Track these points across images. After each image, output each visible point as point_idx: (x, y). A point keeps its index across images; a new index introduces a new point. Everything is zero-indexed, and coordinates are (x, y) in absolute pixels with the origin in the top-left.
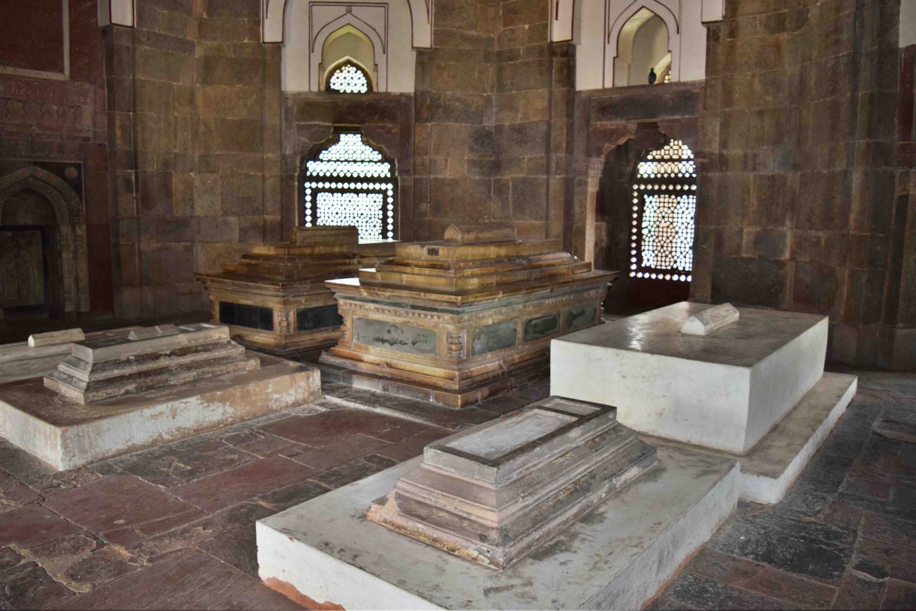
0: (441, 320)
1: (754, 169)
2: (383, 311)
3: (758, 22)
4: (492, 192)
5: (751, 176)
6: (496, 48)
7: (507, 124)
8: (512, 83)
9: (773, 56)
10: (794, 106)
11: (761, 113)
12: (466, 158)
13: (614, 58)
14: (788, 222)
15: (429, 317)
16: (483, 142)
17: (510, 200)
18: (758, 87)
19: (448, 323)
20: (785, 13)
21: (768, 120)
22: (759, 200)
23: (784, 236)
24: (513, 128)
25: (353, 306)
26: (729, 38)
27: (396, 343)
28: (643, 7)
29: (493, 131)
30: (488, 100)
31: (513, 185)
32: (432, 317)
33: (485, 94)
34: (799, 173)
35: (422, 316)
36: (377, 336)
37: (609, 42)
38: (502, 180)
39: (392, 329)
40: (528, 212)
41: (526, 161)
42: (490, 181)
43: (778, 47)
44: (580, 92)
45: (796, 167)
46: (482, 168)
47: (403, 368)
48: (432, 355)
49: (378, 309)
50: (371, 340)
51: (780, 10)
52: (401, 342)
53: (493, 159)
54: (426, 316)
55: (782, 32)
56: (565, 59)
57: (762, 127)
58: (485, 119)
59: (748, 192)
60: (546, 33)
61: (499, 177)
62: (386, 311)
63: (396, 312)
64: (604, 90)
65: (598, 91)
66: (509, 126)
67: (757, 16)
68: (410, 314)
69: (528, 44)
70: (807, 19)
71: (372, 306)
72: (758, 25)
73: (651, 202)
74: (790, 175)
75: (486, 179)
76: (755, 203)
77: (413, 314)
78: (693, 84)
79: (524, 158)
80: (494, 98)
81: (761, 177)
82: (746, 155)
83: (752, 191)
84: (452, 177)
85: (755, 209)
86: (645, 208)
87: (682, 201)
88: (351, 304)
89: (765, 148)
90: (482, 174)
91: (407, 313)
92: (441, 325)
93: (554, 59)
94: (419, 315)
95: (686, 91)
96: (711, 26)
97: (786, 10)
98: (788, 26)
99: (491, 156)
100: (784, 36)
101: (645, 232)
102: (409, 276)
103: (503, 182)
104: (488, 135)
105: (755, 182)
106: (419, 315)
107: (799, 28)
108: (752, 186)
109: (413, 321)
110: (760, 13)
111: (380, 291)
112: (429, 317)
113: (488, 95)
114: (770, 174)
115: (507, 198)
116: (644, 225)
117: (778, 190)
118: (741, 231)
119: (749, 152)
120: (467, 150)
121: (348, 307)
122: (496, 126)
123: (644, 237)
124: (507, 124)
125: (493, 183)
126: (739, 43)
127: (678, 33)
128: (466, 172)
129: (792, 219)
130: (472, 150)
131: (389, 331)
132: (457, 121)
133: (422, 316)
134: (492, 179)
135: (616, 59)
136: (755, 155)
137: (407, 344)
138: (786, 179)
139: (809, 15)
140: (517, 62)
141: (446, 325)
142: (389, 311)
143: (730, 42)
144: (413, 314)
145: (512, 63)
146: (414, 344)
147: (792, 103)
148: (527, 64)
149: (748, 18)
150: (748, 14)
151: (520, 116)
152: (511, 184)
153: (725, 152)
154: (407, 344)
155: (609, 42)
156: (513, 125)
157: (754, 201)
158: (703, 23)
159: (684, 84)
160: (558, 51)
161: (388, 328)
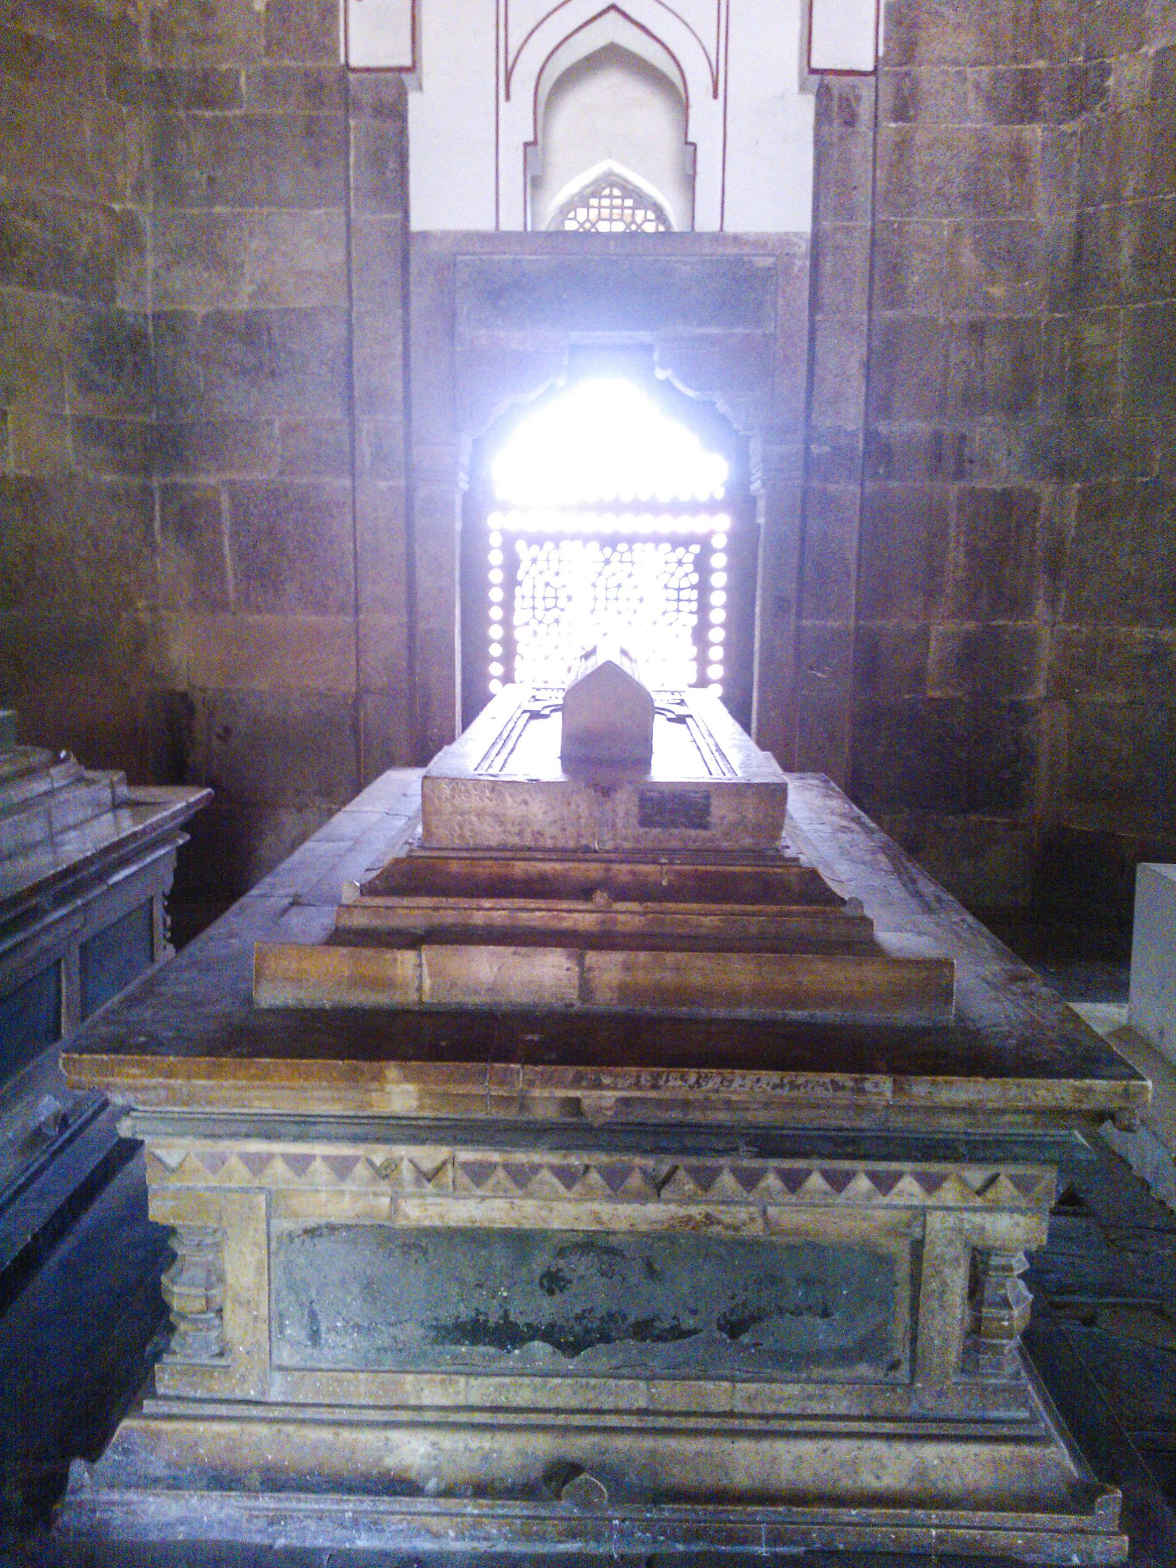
0: (949, 1194)
1: (959, 474)
2: (521, 1177)
3: (969, 86)
4: (157, 524)
5: (955, 489)
6: (146, 57)
7: (199, 309)
8: (211, 180)
9: (1007, 183)
10: (1057, 315)
11: (977, 330)
12: (68, 411)
13: (526, 145)
14: (1040, 606)
15: (862, 1184)
16: (120, 365)
17: (227, 551)
18: (968, 259)
19: (993, 1208)
20: (1039, 71)
21: (993, 347)
22: (972, 552)
23: (1029, 641)
24: (220, 322)
25: (279, 1167)
26: (895, 121)
27: (606, 1339)
28: (613, 7)
29: (151, 330)
30: (129, 229)
31: (236, 506)
32: (884, 1183)
33: (117, 207)
34: (1077, 485)
35: (816, 1181)
36: (465, 1312)
37: (508, 97)
38: (194, 487)
39: (581, 1266)
40: (291, 589)
41: (276, 432)
42: (147, 490)
43: (1019, 157)
44: (425, 235)
45: (1062, 471)
46: (121, 445)
47: (709, 1479)
48: (863, 1369)
49: (479, 1173)
50: (412, 1333)
51: (1027, 62)
52: (643, 1330)
53: (152, 418)
54: (838, 1181)
55: (1031, 120)
56: (390, 126)
57: (981, 366)
58: (121, 286)
59: (945, 536)
60: (329, 32)
61: (180, 479)
62: (546, 1174)
63: (615, 1179)
64: (497, 238)
65: (483, 237)
66: (206, 318)
67: (969, 70)
68: (727, 1180)
69: (266, 62)
70: (1102, 92)
71: (430, 1155)
72: (972, 96)
73: (534, 561)
74: (1046, 491)
75: (137, 481)
76: (962, 559)
77: (749, 1180)
78: (760, 243)
79: (269, 423)
80: (146, 222)
81: (973, 494)
82: (938, 436)
83: (952, 532)
84: (27, 472)
85: (960, 573)
86: (520, 575)
87: (616, 557)
88: (258, 1163)
89: (989, 419)
90: (123, 467)
91: (705, 1179)
92: (935, 1221)
93: (352, 123)
94: (793, 1181)
95: (738, 261)
96: (832, 80)
97: (1042, 64)
98: (1045, 106)
99: (144, 410)
100: (1035, 133)
101: (518, 634)
102: (643, 956)
103: (197, 494)
104: (136, 341)
105: (960, 508)
106: (793, 1181)
107: (1074, 115)
108: (953, 518)
109: (743, 1213)
110: (976, 63)
111: (547, 1082)
112: (862, 1184)
113: (130, 213)
114: (998, 487)
115: (216, 546)
116: (518, 619)
117: (1019, 526)
118: (925, 632)
119: (947, 431)
120: (70, 388)
121: (241, 1174)
122: (157, 317)
123: (520, 649)
124: (199, 309)
125: (157, 495)
126: (921, 138)
127: (715, 96)
128: (71, 456)
129: (1053, 602)
130: (87, 386)
131: (553, 1282)
132: (31, 279)
133: (816, 1181)
134: (156, 482)
135: (529, 149)
136: (963, 438)
137: (677, 1333)
138: (1038, 500)
139: (1111, 82)
140: (227, 113)
141: (977, 1219)
142: (568, 1177)
143: (898, 131)
144: (749, 1180)
145: (208, 114)
146: (734, 1328)
147: (1053, 308)
148: (267, 121)
149: (946, 73)
150: (942, 60)
151: (247, 289)
152: (225, 499)
153: (883, 428)
154: (690, 1333)
155: (508, 97)
156: (219, 312)
157: (956, 555)
158: (813, 71)
159: (736, 239)
160: (366, 98)
161: (541, 1261)
